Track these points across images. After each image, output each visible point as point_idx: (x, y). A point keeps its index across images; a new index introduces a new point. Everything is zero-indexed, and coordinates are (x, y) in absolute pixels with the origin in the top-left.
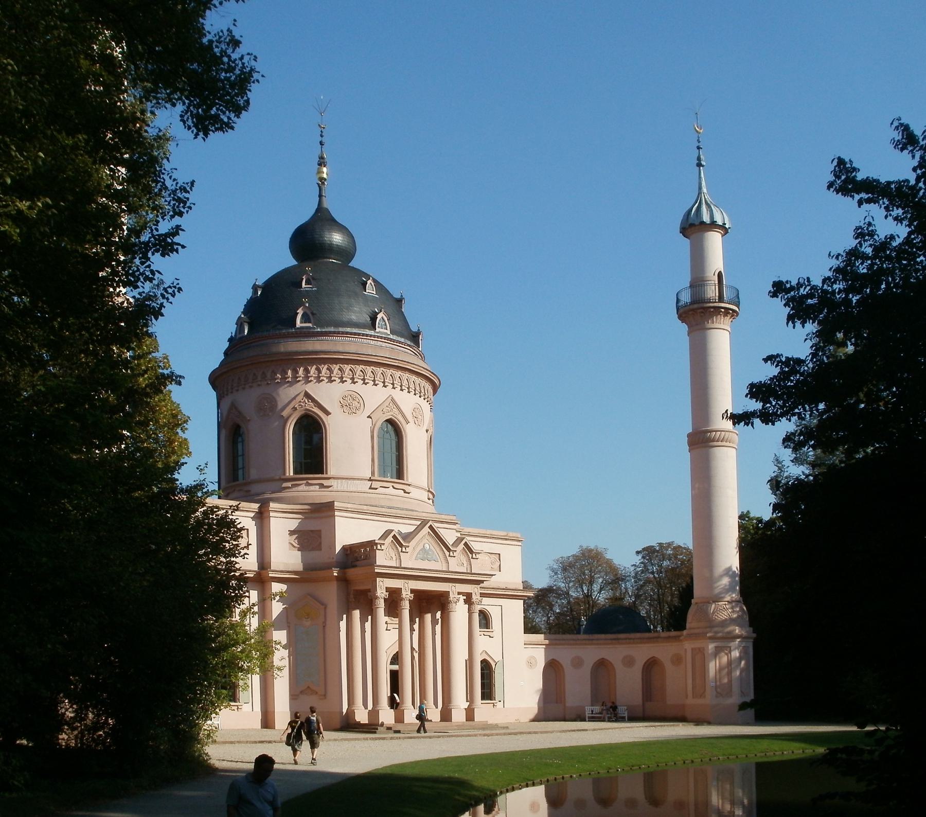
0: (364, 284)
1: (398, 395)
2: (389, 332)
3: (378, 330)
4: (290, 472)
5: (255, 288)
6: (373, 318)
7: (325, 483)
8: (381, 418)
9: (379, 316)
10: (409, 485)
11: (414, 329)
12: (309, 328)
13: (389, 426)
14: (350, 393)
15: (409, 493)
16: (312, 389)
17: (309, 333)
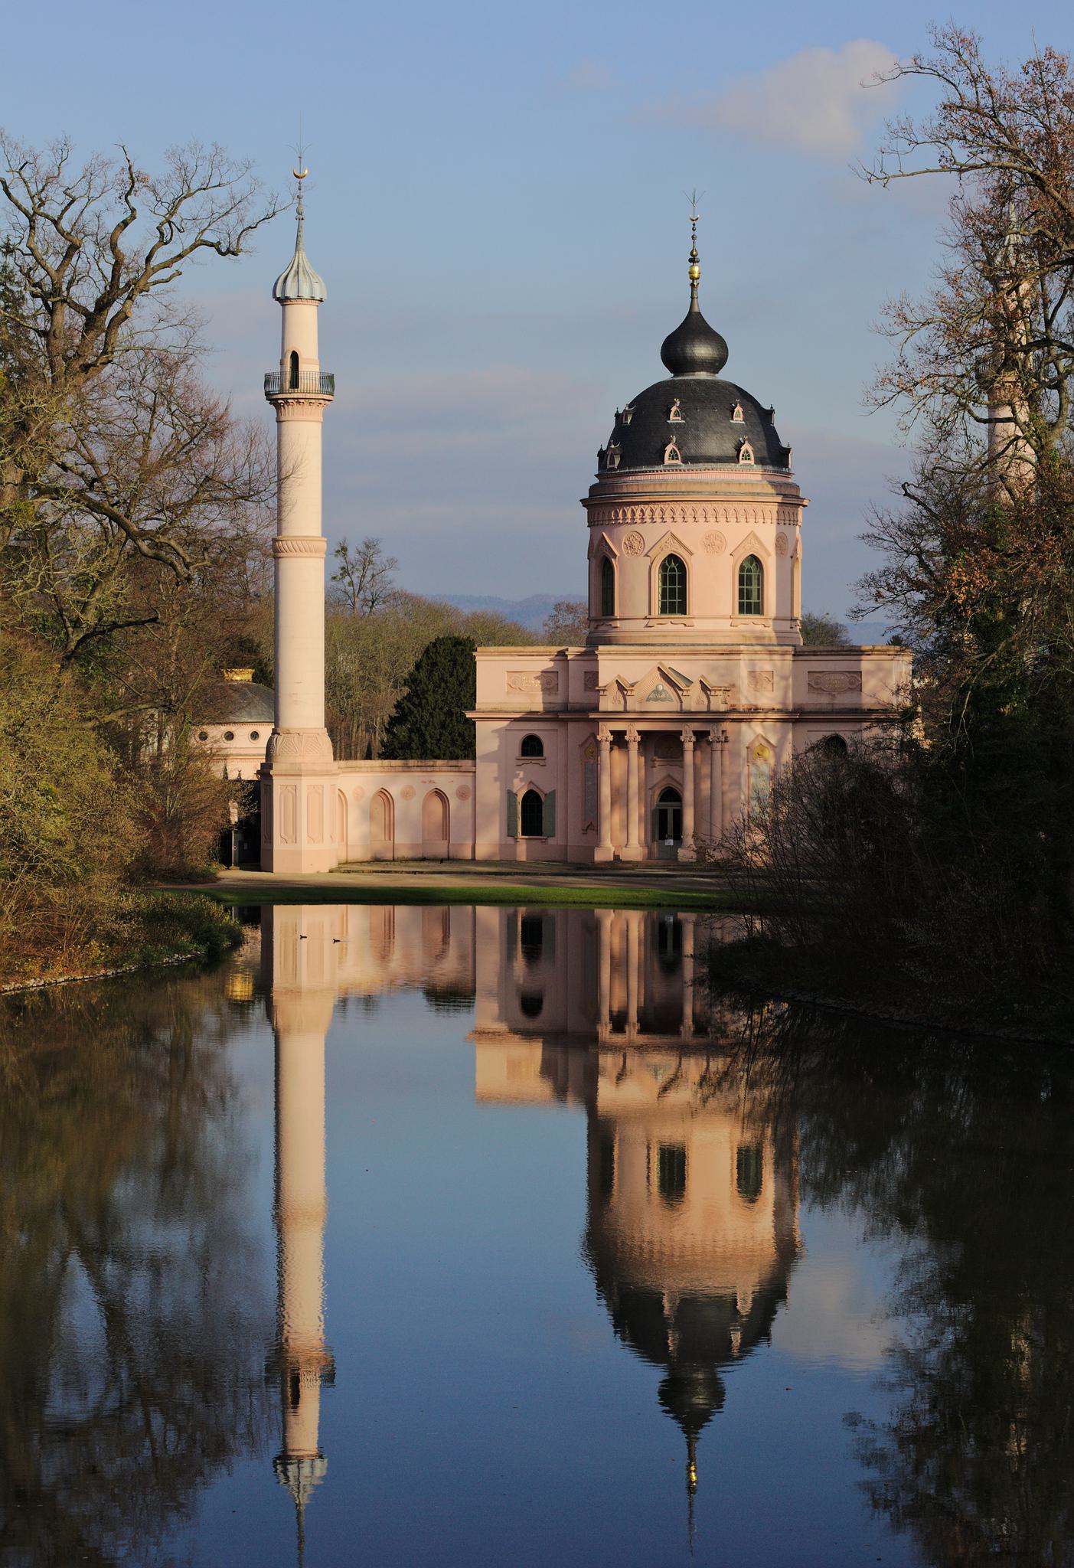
2: (752, 462)
6: (738, 450)
9: (743, 448)
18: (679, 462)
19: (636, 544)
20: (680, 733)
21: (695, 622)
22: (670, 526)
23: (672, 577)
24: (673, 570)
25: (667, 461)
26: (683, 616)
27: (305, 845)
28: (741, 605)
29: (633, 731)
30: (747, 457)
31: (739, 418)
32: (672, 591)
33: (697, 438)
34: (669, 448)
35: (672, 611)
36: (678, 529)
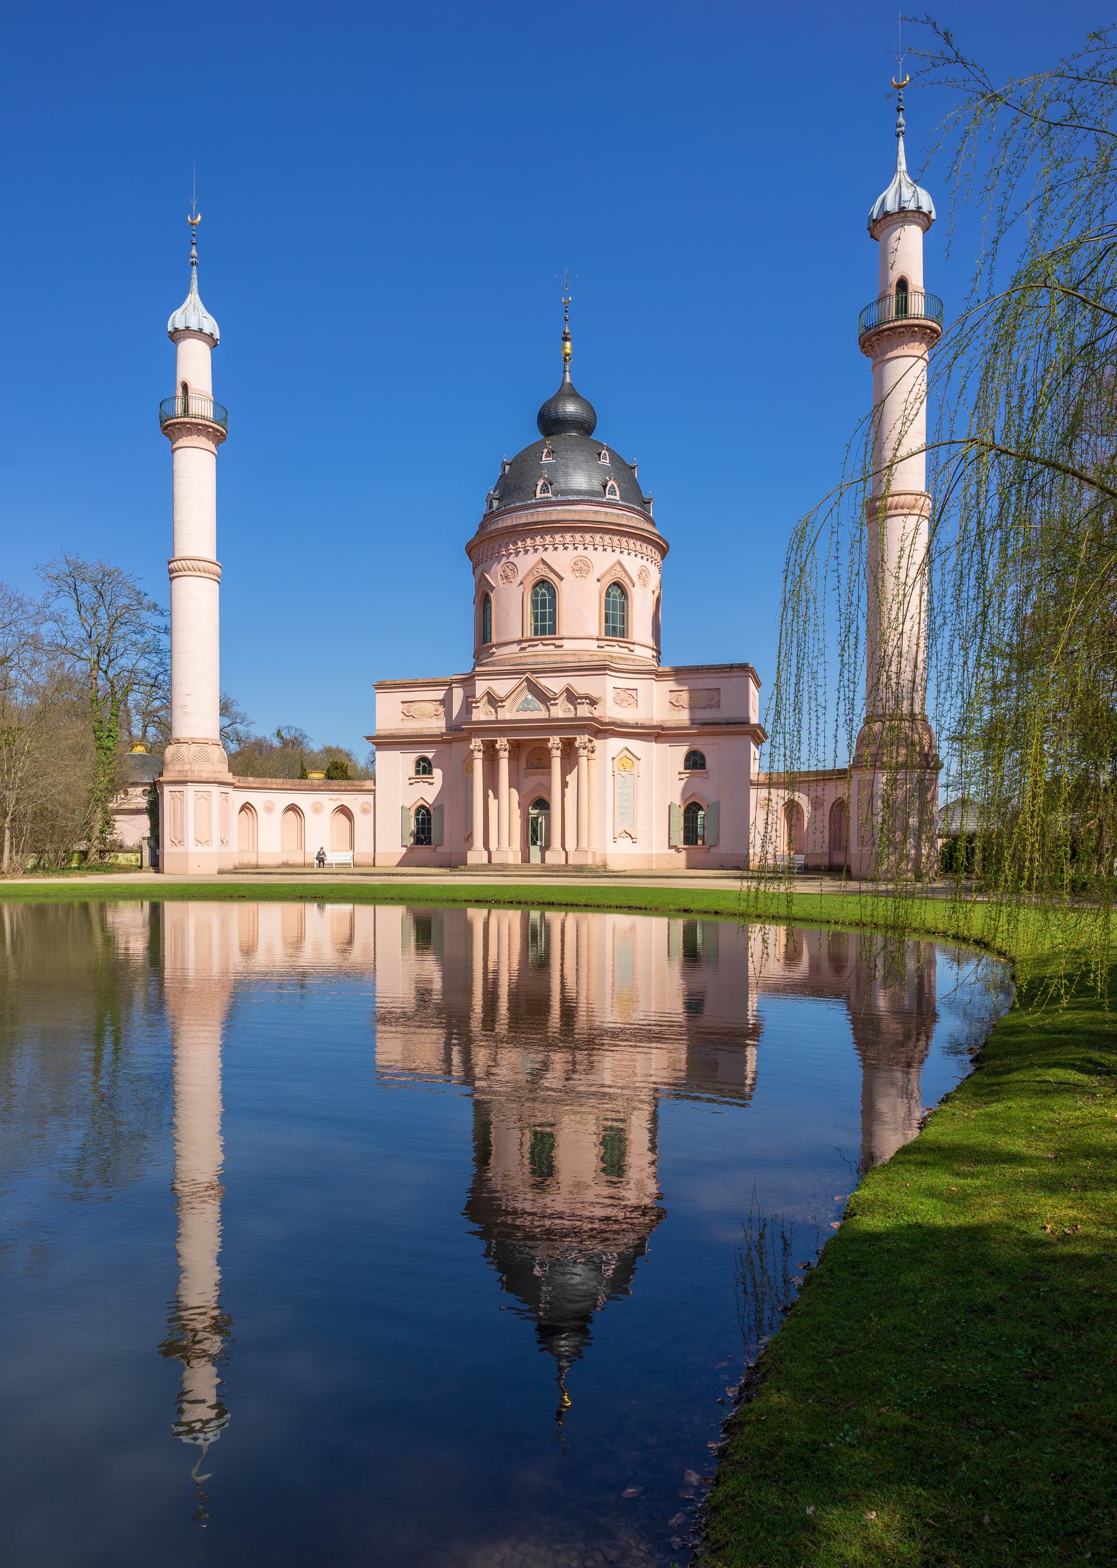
0: (599, 454)
1: (625, 559)
2: (618, 498)
3: (608, 496)
4: (529, 633)
5: (504, 464)
6: (605, 487)
7: (557, 642)
8: (608, 581)
9: (609, 484)
10: (634, 644)
11: (646, 496)
12: (548, 498)
13: (615, 588)
14: (581, 558)
15: (633, 651)
16: (549, 556)
17: (547, 502)
18: (549, 495)
19: (509, 573)
20: (548, 740)
21: (564, 642)
22: (541, 553)
23: (543, 602)
24: (543, 595)
25: (539, 495)
26: (552, 636)
27: (191, 847)
28: (607, 628)
29: (502, 742)
30: (613, 493)
31: (606, 462)
32: (543, 614)
33: (566, 474)
34: (540, 483)
35: (543, 633)
36: (549, 556)
